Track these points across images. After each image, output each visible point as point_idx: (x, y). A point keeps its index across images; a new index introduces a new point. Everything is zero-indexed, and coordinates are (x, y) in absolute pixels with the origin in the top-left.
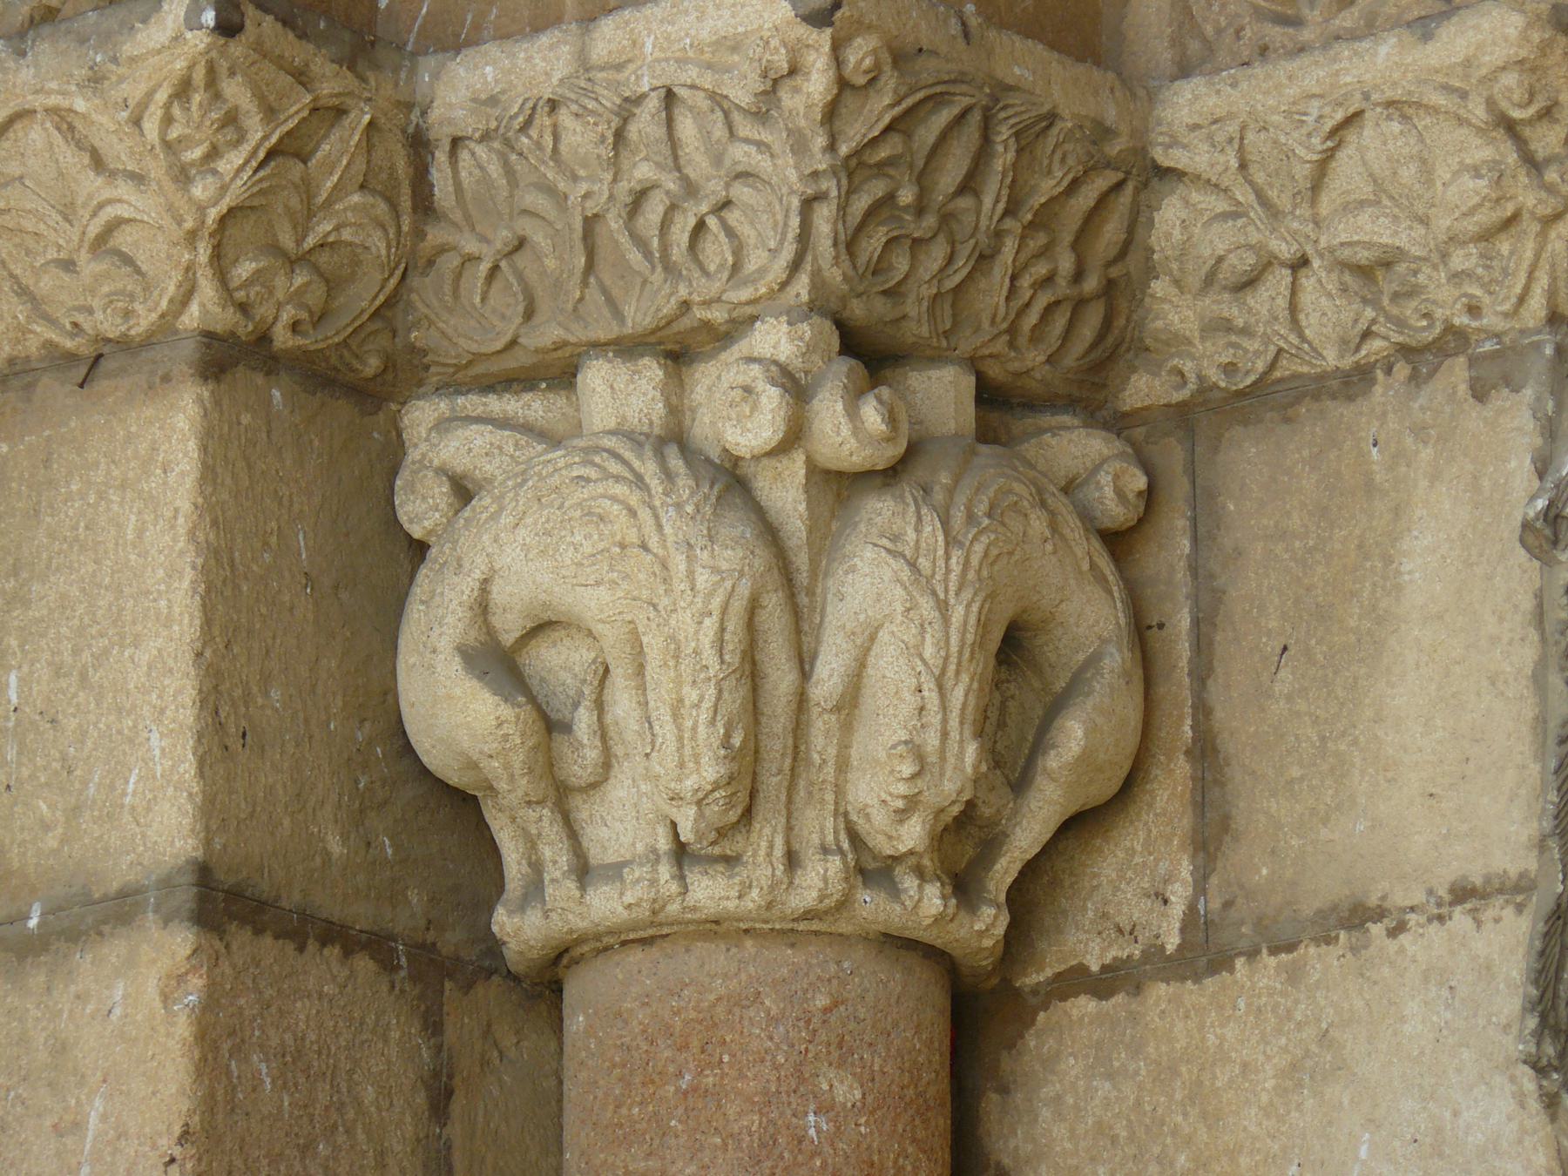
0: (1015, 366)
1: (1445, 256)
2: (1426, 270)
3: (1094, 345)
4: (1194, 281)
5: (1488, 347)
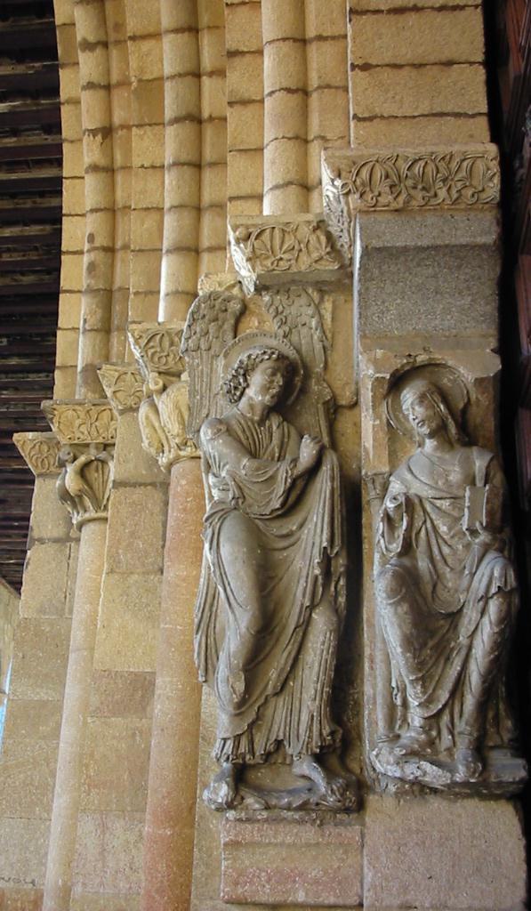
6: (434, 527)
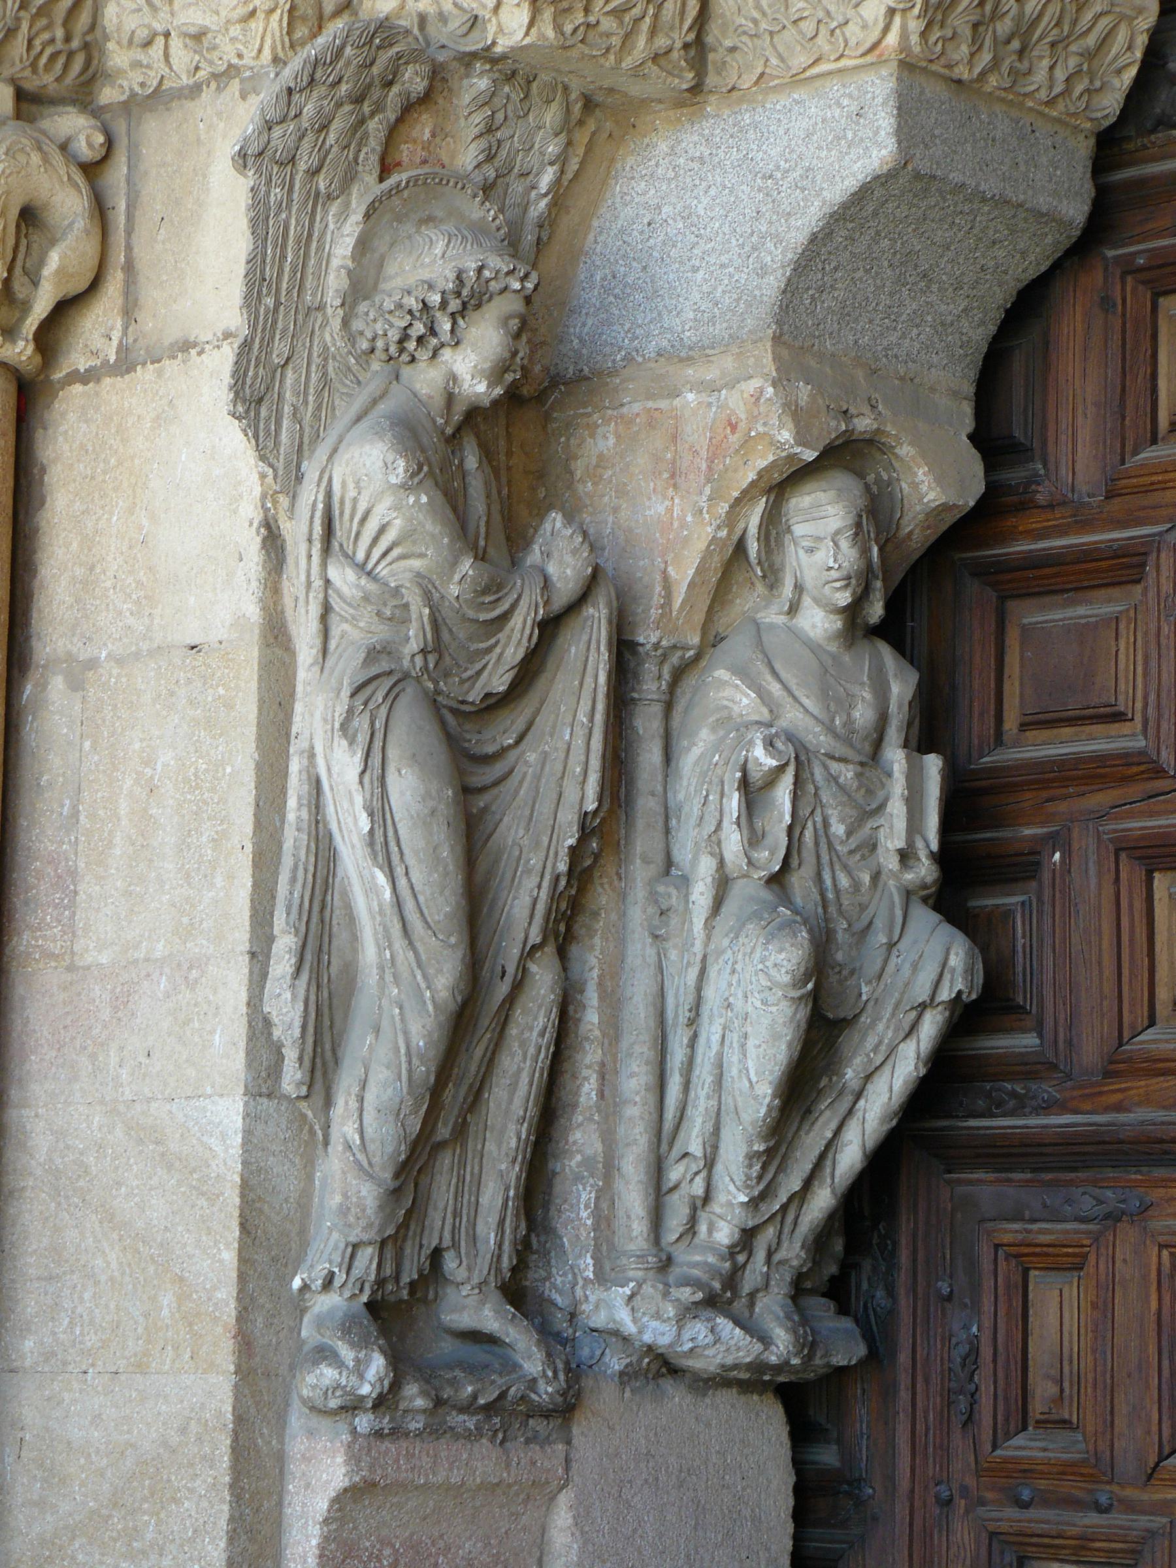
0: (38, 83)
1: (227, 30)
2: (220, 36)
3: (82, 73)
4: (125, 42)
5: (248, 74)
6: (826, 824)
